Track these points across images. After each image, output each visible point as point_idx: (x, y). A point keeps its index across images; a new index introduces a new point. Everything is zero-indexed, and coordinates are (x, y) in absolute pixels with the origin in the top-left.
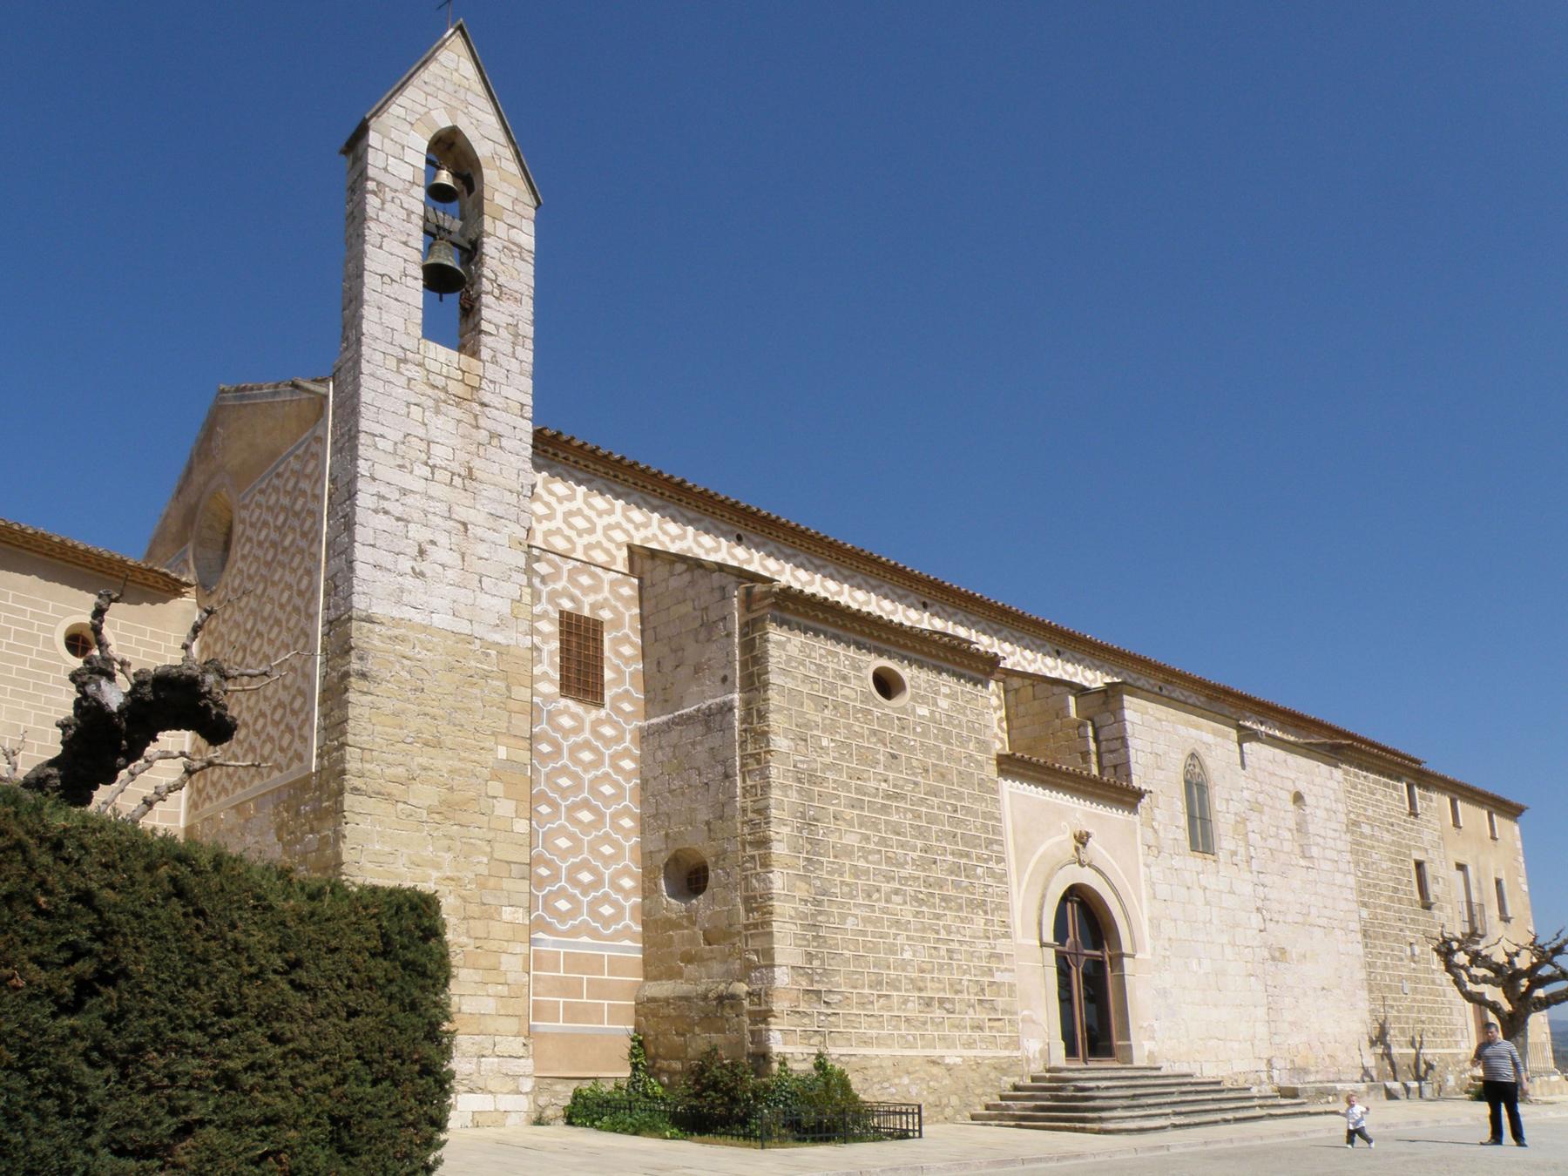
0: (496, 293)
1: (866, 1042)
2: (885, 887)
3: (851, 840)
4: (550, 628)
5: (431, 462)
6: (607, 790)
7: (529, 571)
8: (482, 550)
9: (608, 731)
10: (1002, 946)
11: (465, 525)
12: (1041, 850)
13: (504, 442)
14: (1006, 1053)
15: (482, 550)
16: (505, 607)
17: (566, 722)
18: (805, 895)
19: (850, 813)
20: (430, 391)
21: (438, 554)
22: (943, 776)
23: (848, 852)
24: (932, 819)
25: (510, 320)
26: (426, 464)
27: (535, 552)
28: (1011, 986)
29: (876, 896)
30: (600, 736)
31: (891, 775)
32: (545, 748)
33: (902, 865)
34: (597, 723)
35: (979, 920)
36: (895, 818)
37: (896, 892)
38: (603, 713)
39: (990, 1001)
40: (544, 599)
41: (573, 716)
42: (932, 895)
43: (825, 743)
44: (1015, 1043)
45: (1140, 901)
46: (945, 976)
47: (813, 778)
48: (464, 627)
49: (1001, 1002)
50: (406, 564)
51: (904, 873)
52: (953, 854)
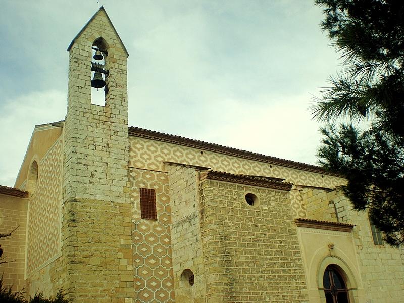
0: (115, 85)
3: (242, 259)
4: (137, 195)
5: (95, 144)
6: (160, 250)
7: (129, 176)
8: (112, 171)
9: (159, 229)
10: (303, 292)
11: (107, 163)
12: (315, 253)
13: (119, 133)
15: (112, 171)
16: (121, 190)
17: (144, 227)
18: (226, 282)
19: (241, 249)
20: (94, 121)
21: (97, 175)
22: (275, 230)
24: (274, 247)
25: (120, 94)
26: (93, 145)
27: (131, 169)
29: (253, 279)
30: (157, 231)
31: (255, 233)
32: (137, 238)
33: (262, 266)
34: (155, 226)
35: (294, 283)
36: (258, 249)
38: (157, 222)
40: (134, 185)
41: (146, 225)
42: (275, 276)
43: (230, 224)
45: (357, 267)
47: (226, 238)
48: (107, 199)
50: (87, 180)
52: (281, 259)
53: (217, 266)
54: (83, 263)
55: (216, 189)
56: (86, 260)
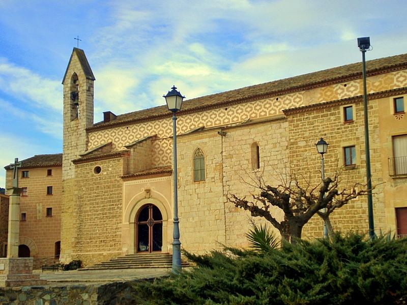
1: (87, 252)
3: (88, 209)
13: (82, 135)
23: (87, 211)
28: (121, 235)
33: (97, 211)
36: (97, 201)
37: (96, 218)
39: (115, 240)
44: (120, 249)
46: (105, 235)
49: (117, 239)
50: (68, 169)
51: (98, 213)
53: (75, 214)
54: (66, 212)
55: (79, 169)
56: (67, 210)
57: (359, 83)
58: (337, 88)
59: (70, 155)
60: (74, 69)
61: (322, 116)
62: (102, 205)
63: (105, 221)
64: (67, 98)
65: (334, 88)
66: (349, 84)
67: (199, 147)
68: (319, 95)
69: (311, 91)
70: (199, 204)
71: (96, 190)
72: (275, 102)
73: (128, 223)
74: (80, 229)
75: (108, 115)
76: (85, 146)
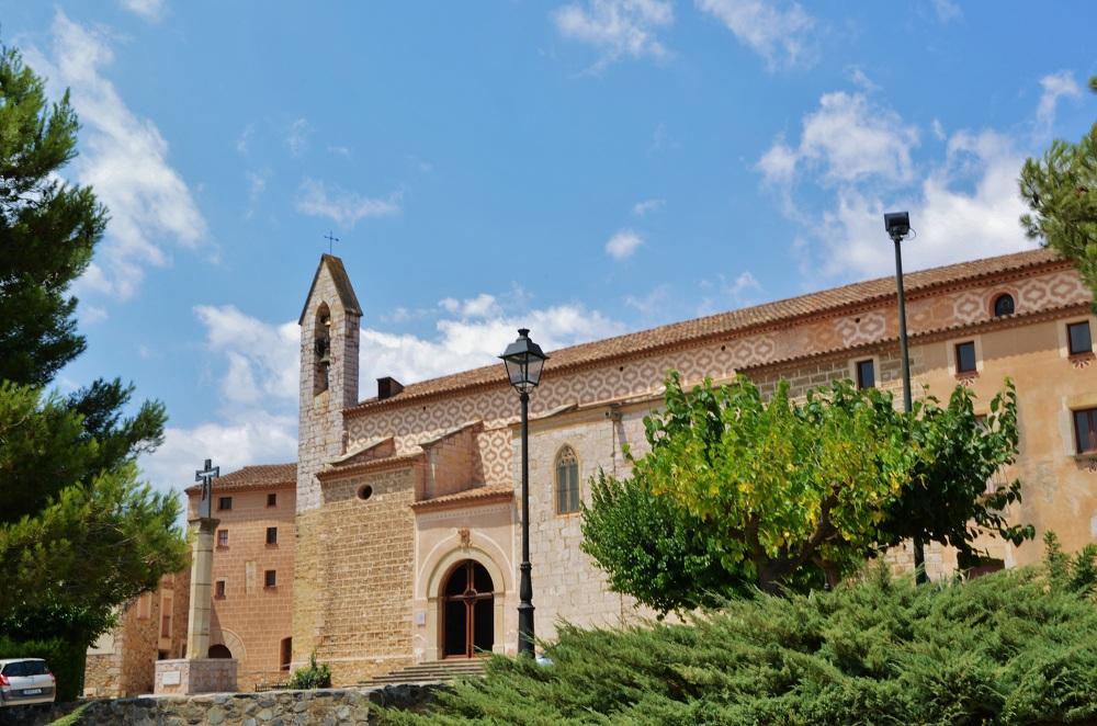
1: (344, 655)
2: (357, 586)
12: (436, 547)
13: (335, 424)
14: (405, 656)
23: (344, 575)
28: (410, 622)
37: (362, 587)
44: (409, 650)
45: (511, 561)
50: (308, 490)
53: (320, 580)
57: (883, 315)
58: (841, 325)
59: (312, 463)
60: (322, 297)
61: (813, 381)
62: (373, 563)
63: (379, 595)
64: (307, 352)
65: (835, 325)
66: (864, 317)
67: (569, 442)
68: (806, 340)
69: (791, 332)
70: (569, 559)
71: (362, 532)
72: (719, 355)
73: (425, 598)
74: (330, 612)
75: (387, 386)
76: (341, 445)
